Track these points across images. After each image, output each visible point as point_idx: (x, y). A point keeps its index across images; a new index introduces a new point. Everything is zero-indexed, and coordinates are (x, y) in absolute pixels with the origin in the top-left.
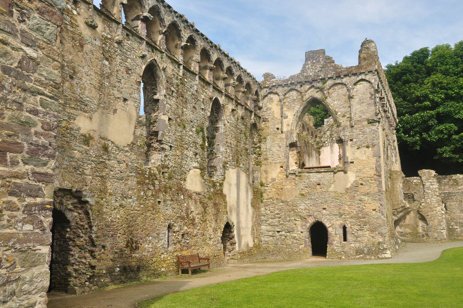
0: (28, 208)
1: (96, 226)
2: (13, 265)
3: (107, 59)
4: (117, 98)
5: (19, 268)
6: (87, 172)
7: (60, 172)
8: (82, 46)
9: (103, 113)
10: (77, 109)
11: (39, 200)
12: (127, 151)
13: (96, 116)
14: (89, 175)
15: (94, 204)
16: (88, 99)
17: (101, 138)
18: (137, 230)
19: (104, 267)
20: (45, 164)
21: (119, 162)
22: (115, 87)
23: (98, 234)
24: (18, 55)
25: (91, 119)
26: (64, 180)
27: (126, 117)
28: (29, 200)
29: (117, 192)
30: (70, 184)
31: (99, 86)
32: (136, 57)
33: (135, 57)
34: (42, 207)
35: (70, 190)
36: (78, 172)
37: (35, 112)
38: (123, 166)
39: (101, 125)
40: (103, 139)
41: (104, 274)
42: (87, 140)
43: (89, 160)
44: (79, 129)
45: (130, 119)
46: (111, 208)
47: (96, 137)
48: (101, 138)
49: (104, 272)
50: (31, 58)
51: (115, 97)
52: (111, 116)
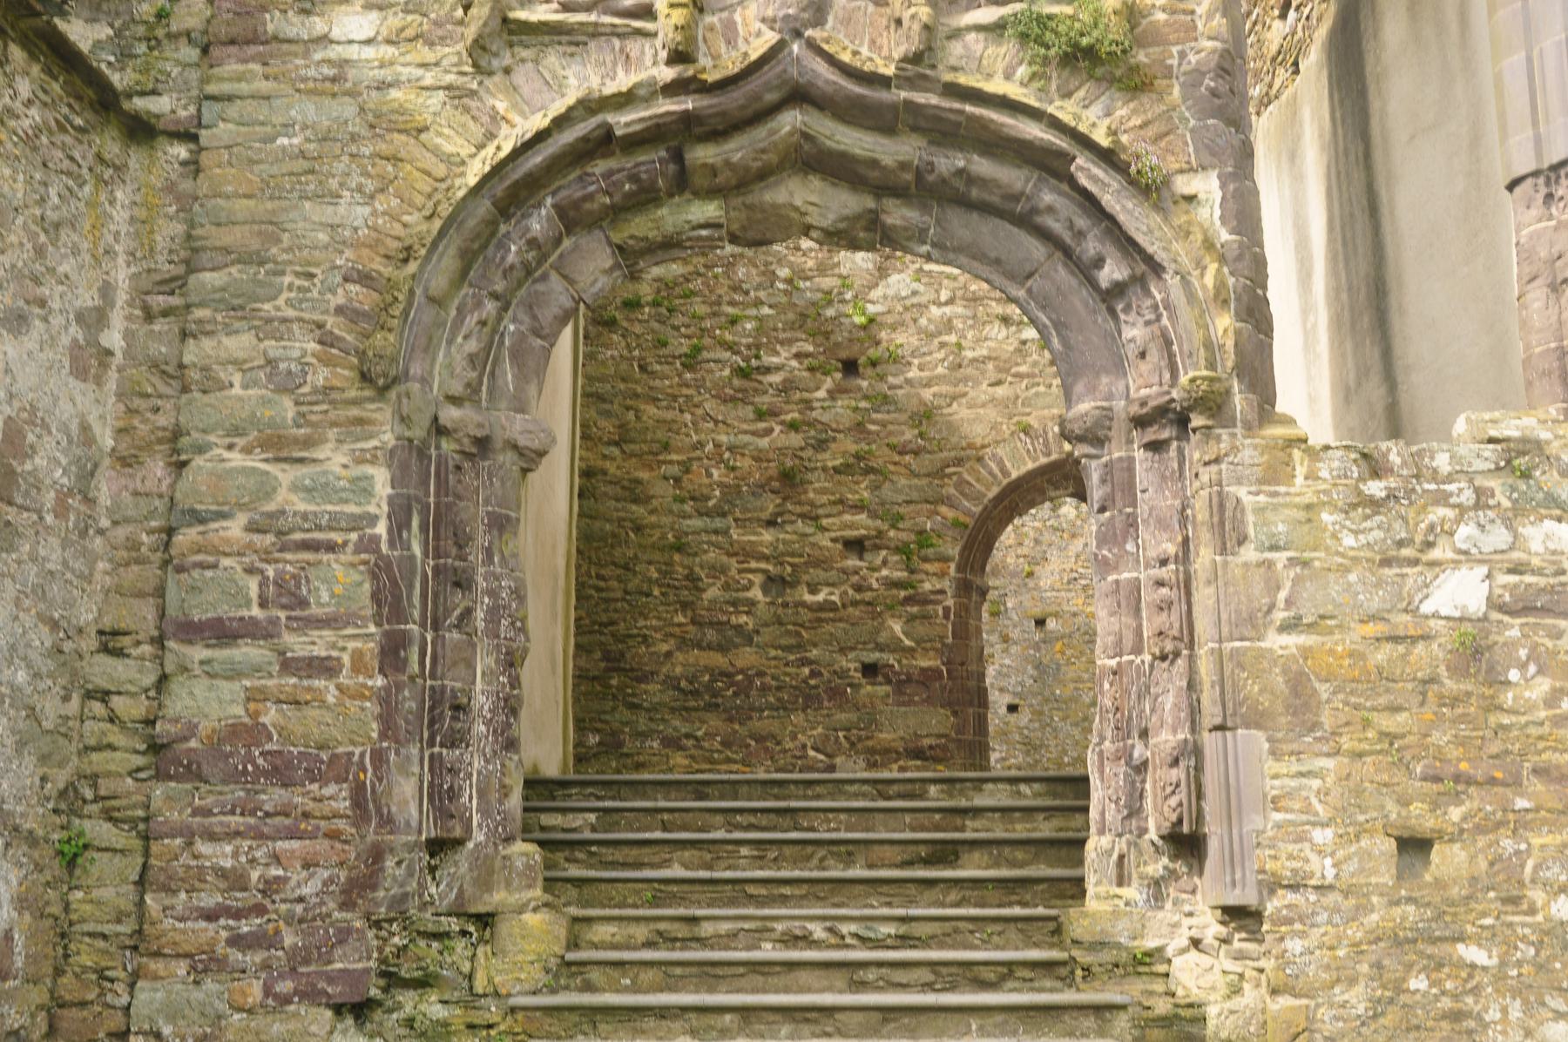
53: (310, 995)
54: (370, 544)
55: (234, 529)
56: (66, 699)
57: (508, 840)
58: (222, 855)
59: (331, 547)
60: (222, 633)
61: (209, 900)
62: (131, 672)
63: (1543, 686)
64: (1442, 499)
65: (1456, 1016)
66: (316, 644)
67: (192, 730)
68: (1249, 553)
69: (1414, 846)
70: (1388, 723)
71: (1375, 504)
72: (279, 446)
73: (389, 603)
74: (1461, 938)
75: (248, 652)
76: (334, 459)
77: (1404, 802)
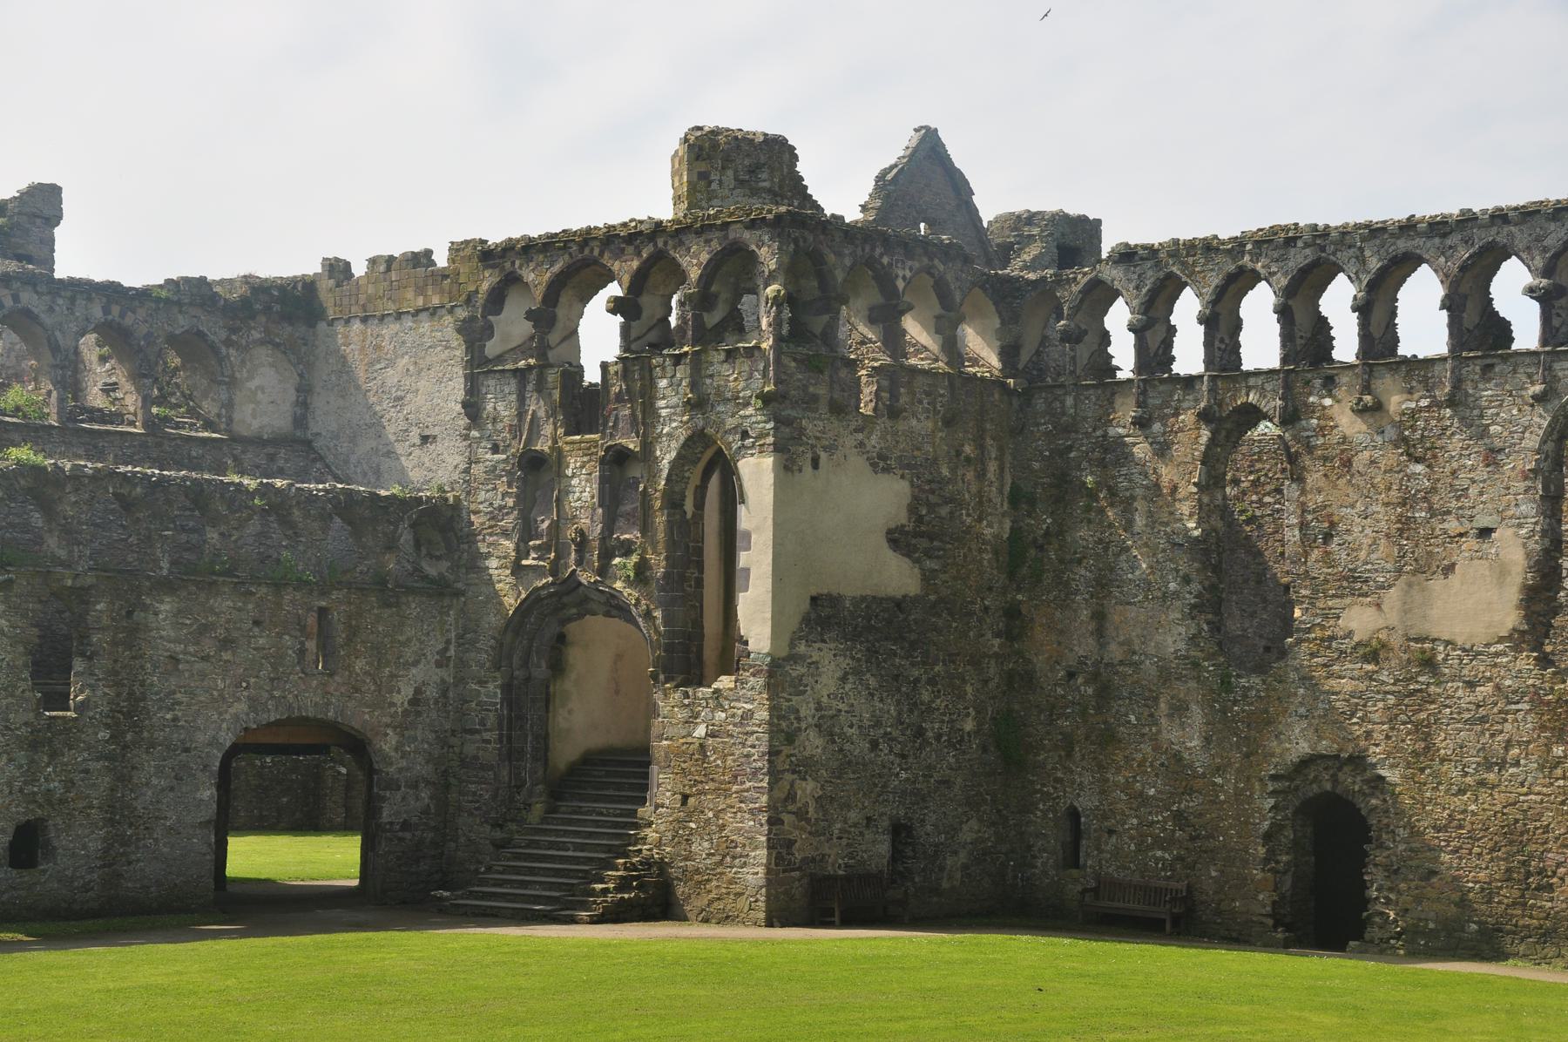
0: (751, 811)
1: (1405, 828)
2: (744, 845)
3: (1418, 460)
4: (1455, 537)
5: (747, 848)
6: (1376, 717)
7: (1310, 725)
8: (1348, 463)
9: (1410, 585)
10: (1342, 596)
11: (757, 805)
12: (1497, 654)
13: (1393, 596)
14: (1378, 723)
15: (1398, 780)
16: (1369, 567)
17: (1409, 640)
18: (1543, 844)
19: (1432, 914)
20: (761, 781)
21: (1471, 685)
22: (1449, 513)
23: (1414, 845)
24: (740, 712)
25: (1378, 606)
26: (1320, 738)
27: (1487, 573)
28: (751, 806)
29: (1467, 753)
30: (1335, 746)
31: (1398, 529)
32: (1520, 410)
33: (1515, 412)
34: (760, 810)
35: (1337, 757)
36: (1355, 720)
37: (753, 746)
38: (1485, 690)
39: (1406, 611)
40: (1417, 640)
41: (1431, 930)
42: (1373, 653)
43: (1378, 692)
44: (1350, 634)
45: (1502, 572)
46: (1449, 789)
47: (1396, 641)
48: (1409, 640)
49: (1431, 925)
50: (749, 710)
51: (1450, 537)
52: (1437, 584)
53: (486, 822)
54: (496, 710)
55: (473, 705)
56: (443, 748)
57: (537, 784)
58: (473, 787)
59: (490, 711)
60: (472, 732)
61: (470, 798)
62: (455, 741)
63: (715, 756)
64: (700, 705)
65: (687, 840)
66: (486, 736)
67: (467, 757)
68: (660, 719)
69: (685, 798)
70: (683, 765)
71: (685, 705)
72: (482, 683)
73: (500, 728)
74: (691, 821)
75: (477, 737)
76: (491, 686)
77: (684, 786)
